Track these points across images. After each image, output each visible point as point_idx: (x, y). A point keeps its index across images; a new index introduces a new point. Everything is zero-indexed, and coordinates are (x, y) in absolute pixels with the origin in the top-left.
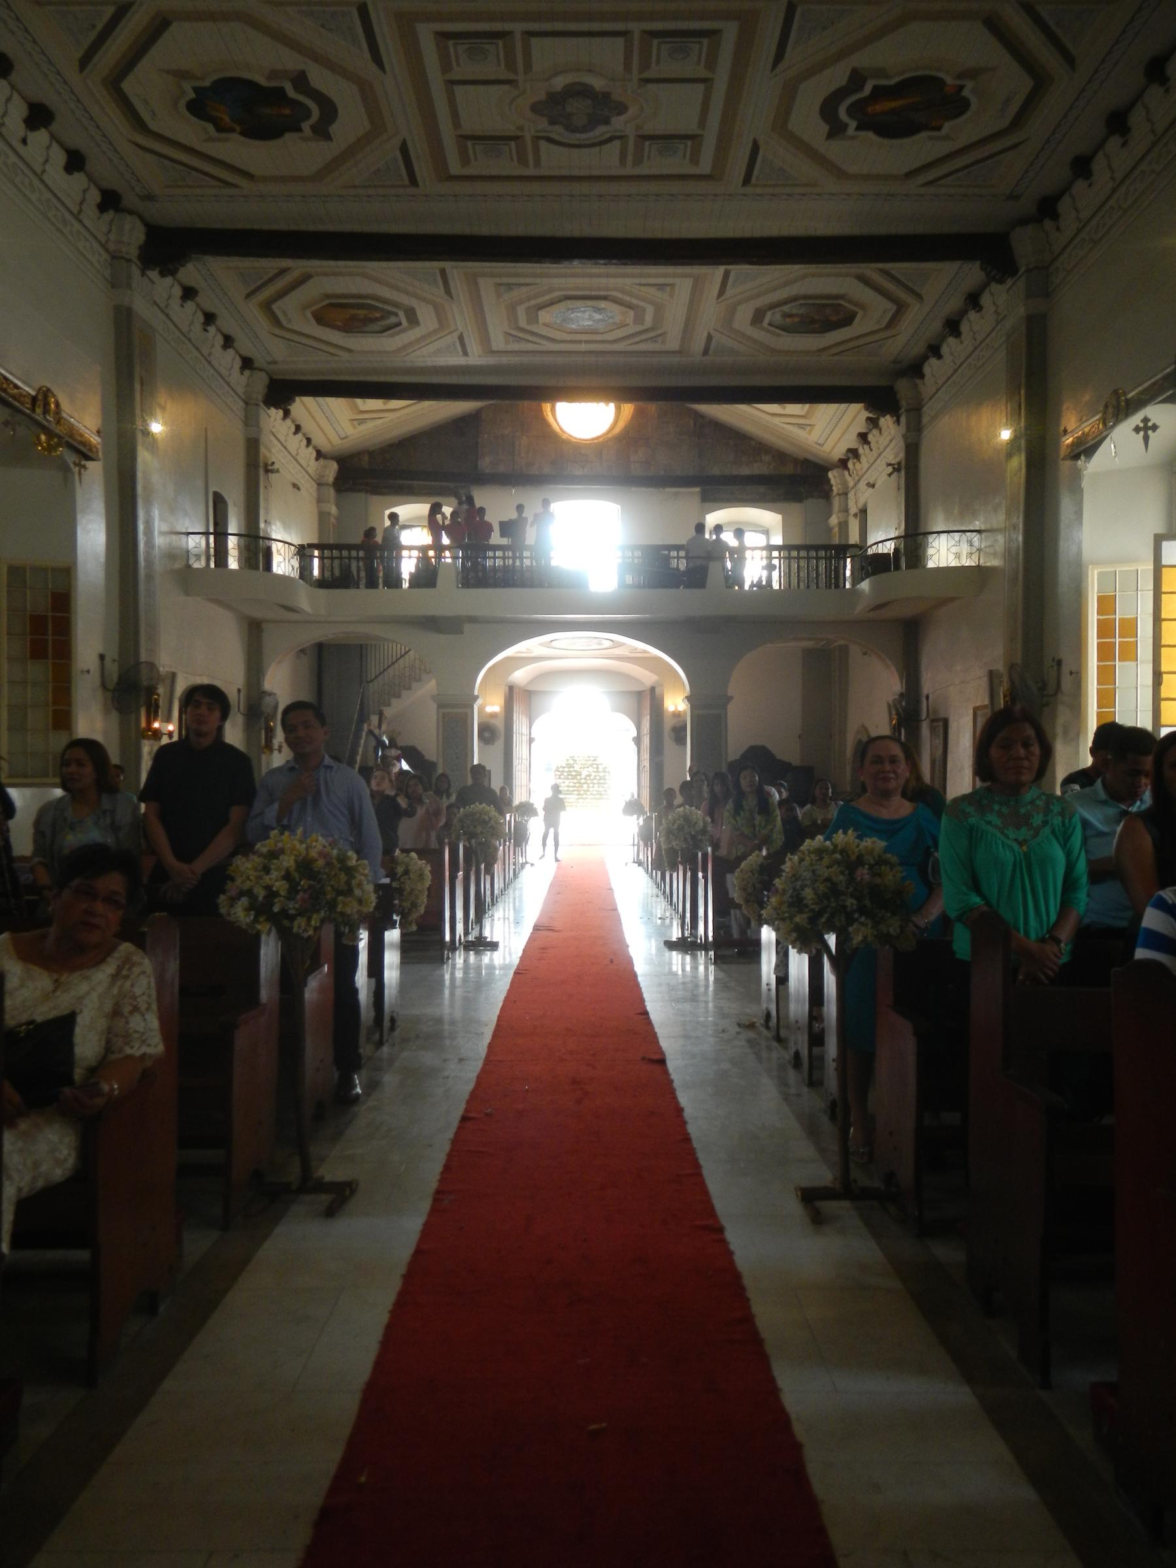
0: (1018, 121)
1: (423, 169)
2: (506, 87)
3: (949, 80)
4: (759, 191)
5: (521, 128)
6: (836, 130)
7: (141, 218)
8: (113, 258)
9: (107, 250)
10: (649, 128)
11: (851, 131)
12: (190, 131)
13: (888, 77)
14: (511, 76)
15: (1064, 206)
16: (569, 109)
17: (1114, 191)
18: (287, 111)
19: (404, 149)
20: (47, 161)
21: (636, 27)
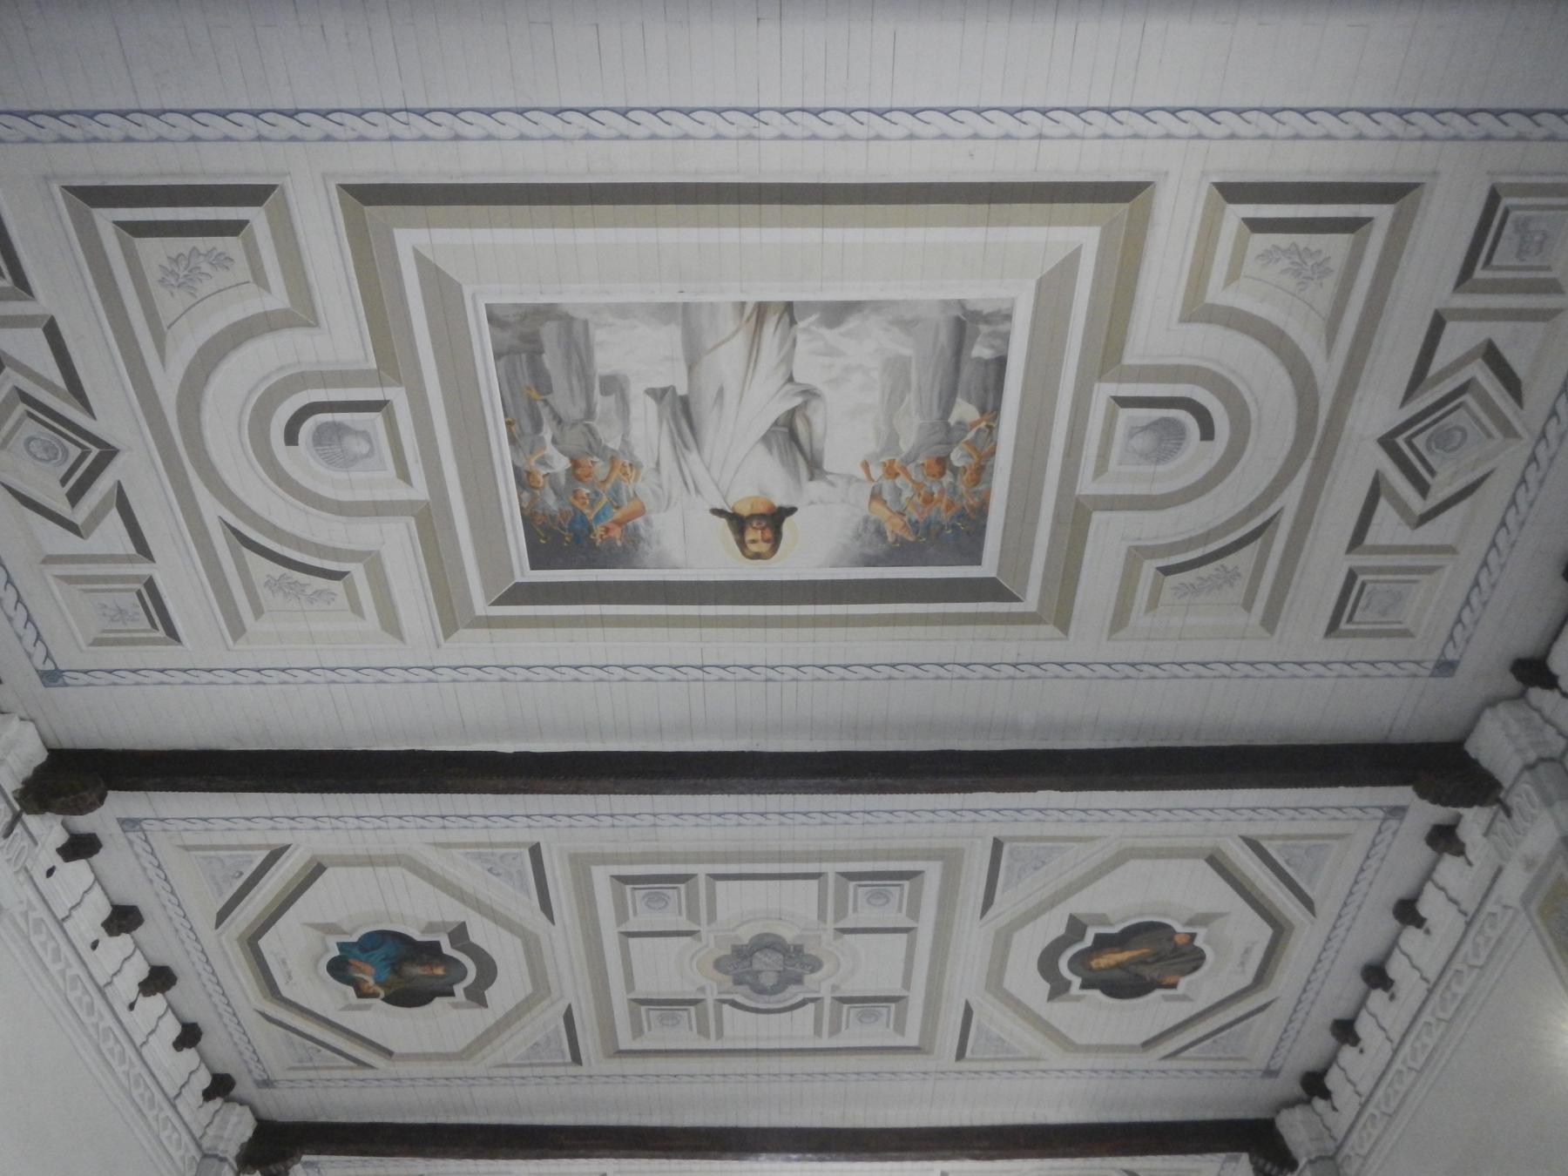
0: (1262, 977)
1: (589, 1042)
3: (1178, 928)
4: (975, 1066)
5: (702, 989)
6: (1059, 989)
7: (254, 1111)
8: (205, 1156)
9: (199, 1146)
10: (848, 990)
12: (330, 998)
13: (1111, 925)
14: (694, 927)
15: (1333, 1080)
16: (756, 966)
17: (1395, 1052)
18: (440, 971)
19: (568, 1018)
20: (153, 1031)
21: (831, 868)
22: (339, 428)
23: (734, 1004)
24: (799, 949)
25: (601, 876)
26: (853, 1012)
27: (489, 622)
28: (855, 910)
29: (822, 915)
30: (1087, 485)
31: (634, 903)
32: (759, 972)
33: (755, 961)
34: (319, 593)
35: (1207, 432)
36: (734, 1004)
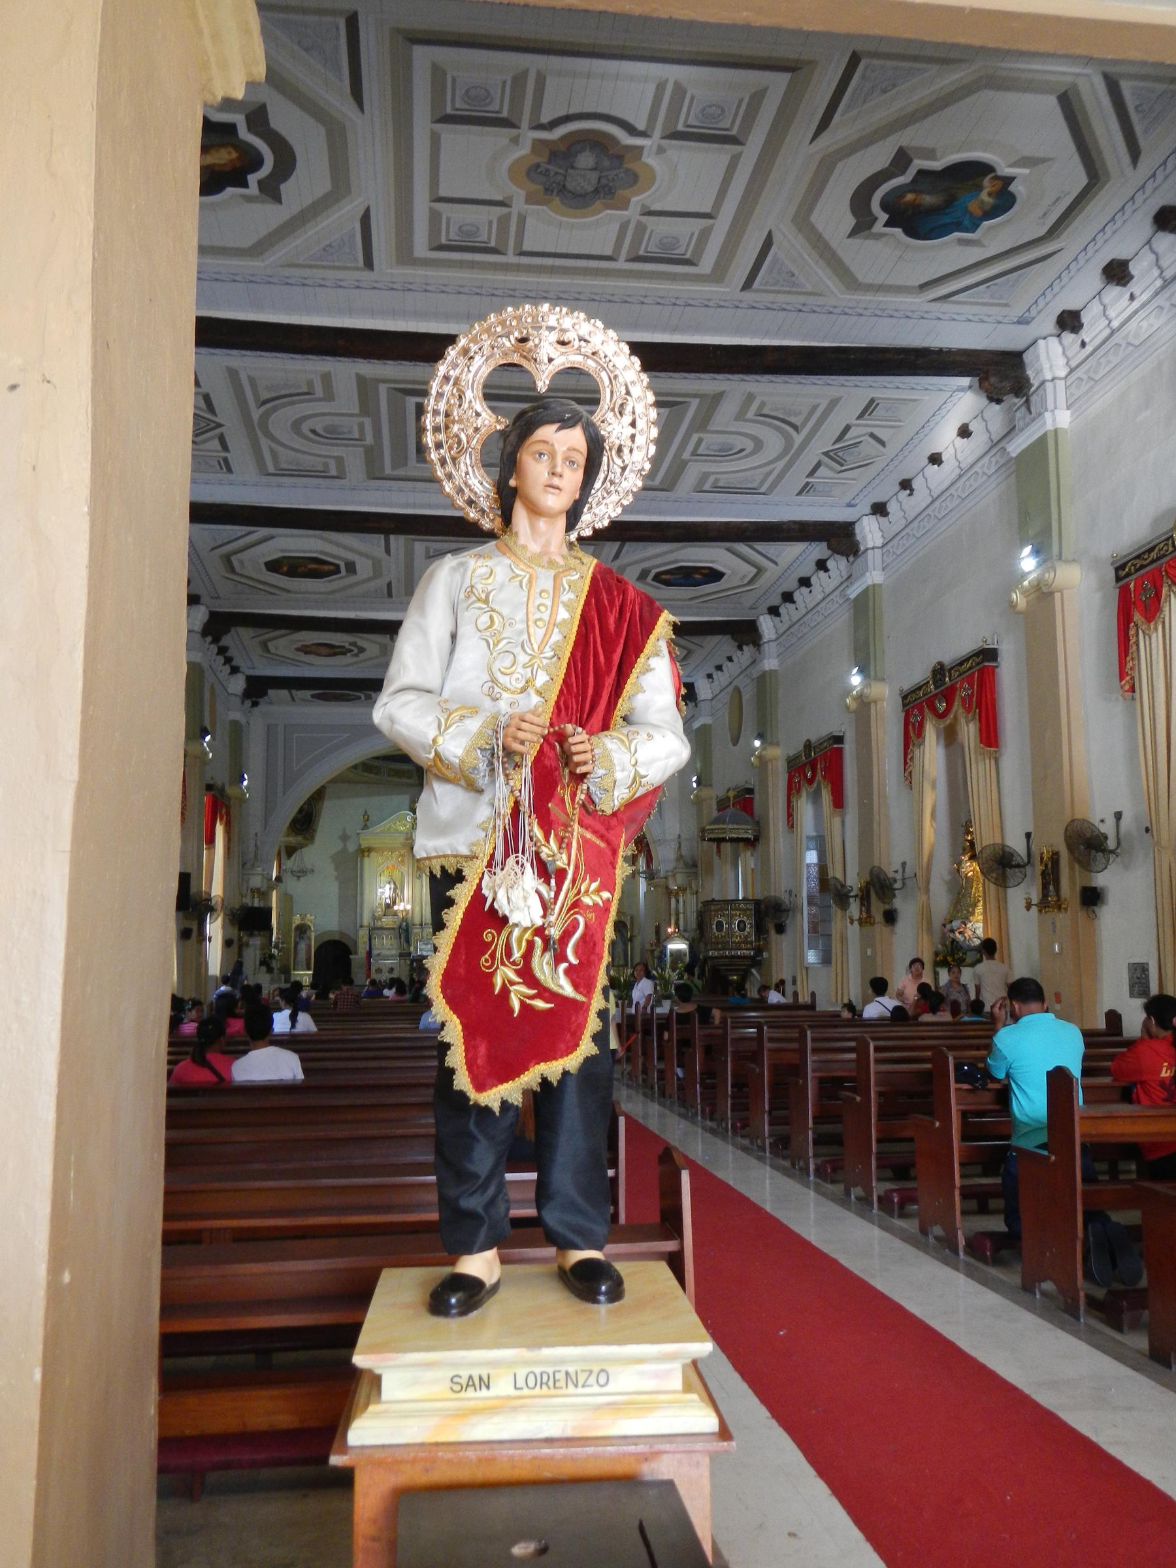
2: (657, 207)
5: (661, 150)
11: (239, 120)
14: (644, 219)
16: (594, 176)
21: (510, 258)
22: (720, 451)
23: (631, 130)
24: (548, 190)
25: (706, 265)
26: (495, 106)
27: (695, 396)
28: (490, 223)
29: (522, 220)
30: (367, 422)
31: (688, 246)
32: (595, 169)
33: (594, 182)
34: (777, 410)
35: (314, 432)
36: (631, 130)
